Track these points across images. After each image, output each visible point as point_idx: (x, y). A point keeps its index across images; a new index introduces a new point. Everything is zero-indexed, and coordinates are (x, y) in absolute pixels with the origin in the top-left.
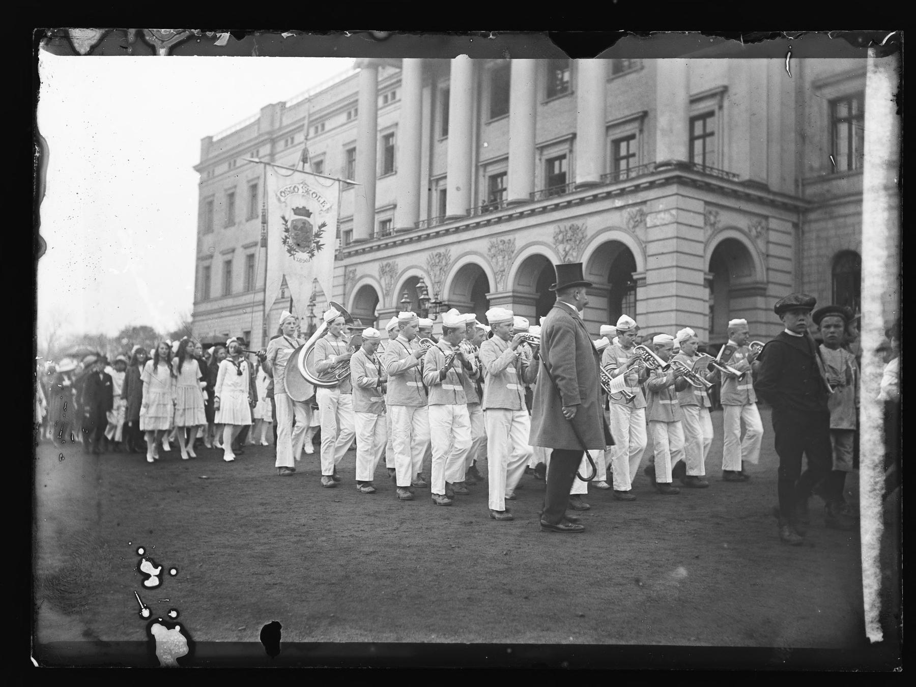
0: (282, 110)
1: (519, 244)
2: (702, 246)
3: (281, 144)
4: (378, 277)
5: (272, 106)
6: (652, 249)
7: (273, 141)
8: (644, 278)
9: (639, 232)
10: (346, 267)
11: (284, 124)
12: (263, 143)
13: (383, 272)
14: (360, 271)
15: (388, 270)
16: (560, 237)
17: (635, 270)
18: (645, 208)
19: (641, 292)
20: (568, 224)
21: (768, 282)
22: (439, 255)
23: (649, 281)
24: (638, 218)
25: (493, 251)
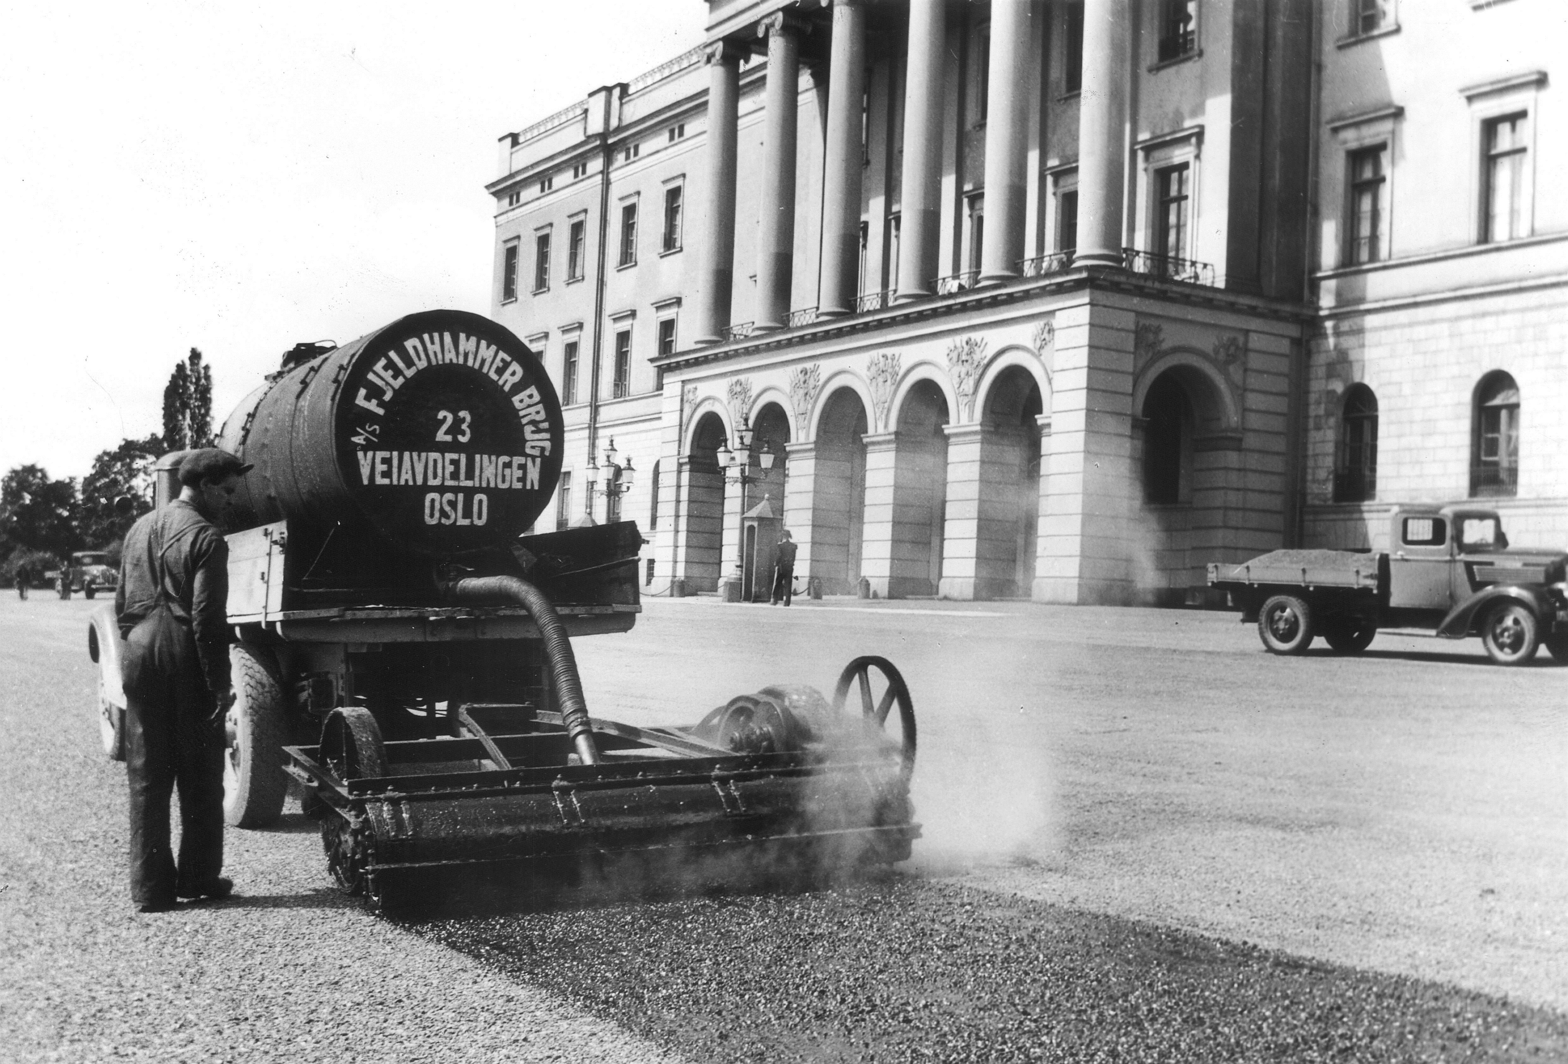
0: (621, 98)
2: (1130, 379)
3: (621, 158)
4: (726, 402)
5: (608, 90)
6: (1058, 379)
10: (683, 382)
11: (626, 121)
13: (733, 394)
14: (704, 390)
15: (739, 392)
16: (954, 355)
17: (1041, 412)
21: (1245, 430)
22: (805, 372)
24: (1046, 335)
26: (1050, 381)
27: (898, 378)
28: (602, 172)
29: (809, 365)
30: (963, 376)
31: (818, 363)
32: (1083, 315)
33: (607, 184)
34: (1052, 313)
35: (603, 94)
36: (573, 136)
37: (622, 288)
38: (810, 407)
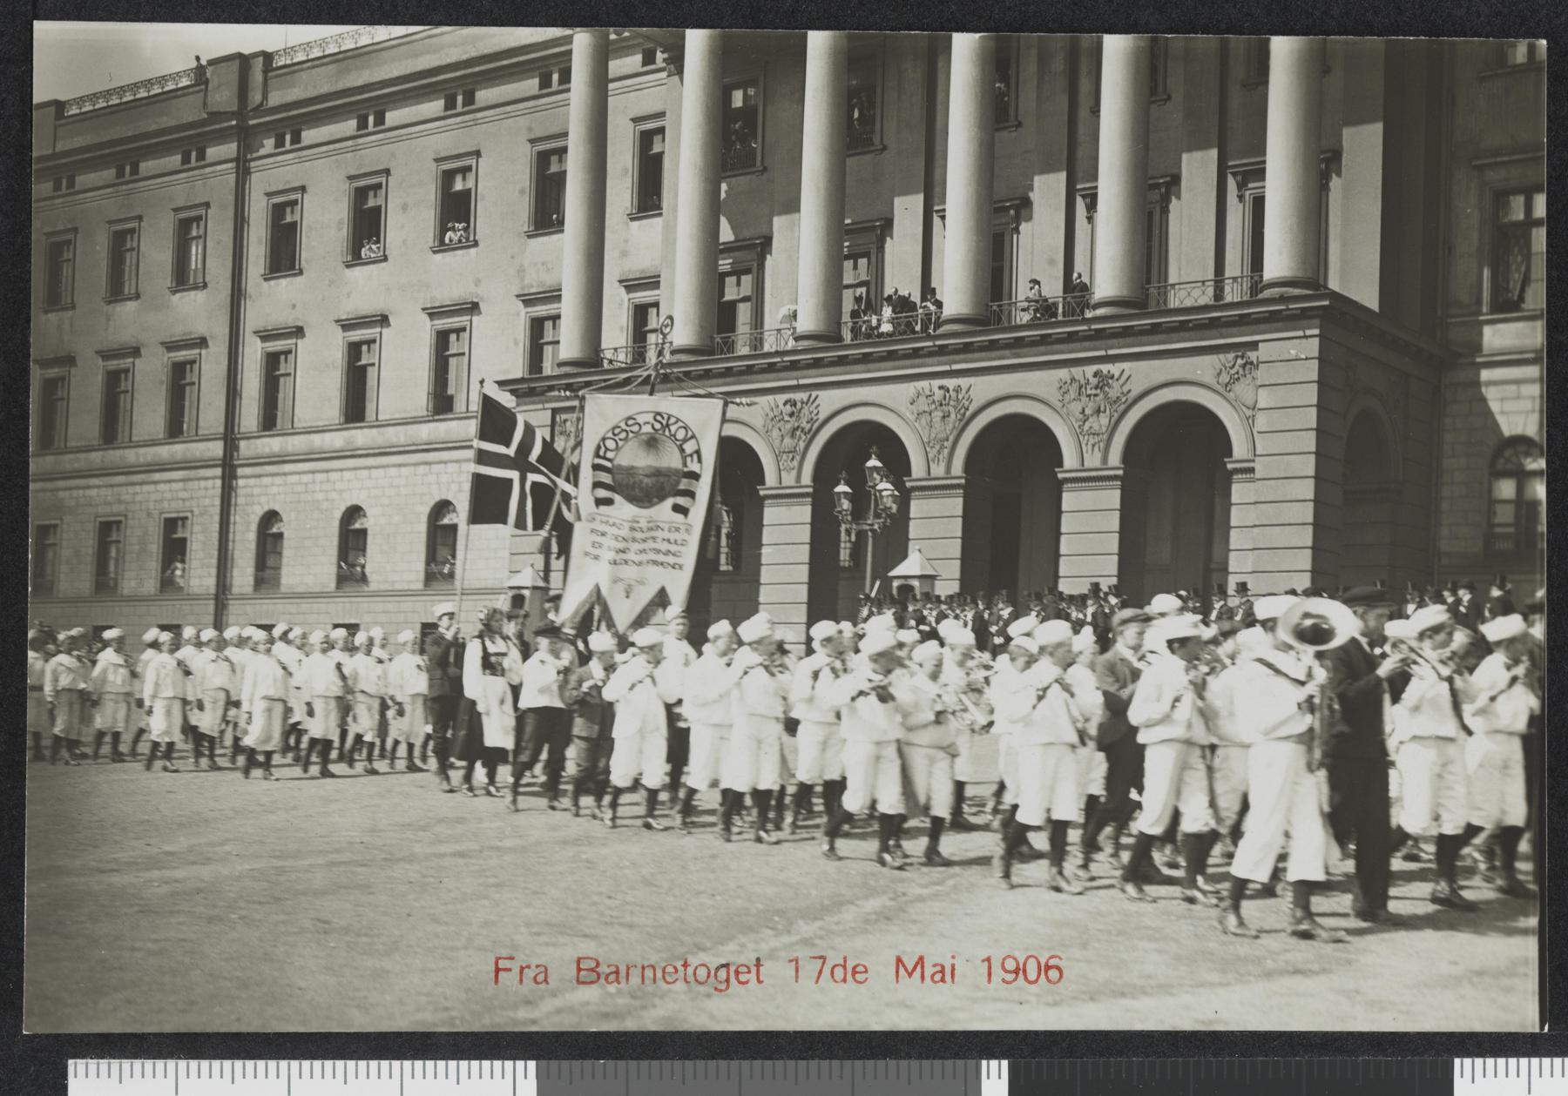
1: (978, 400)
3: (269, 144)
6: (1262, 422)
7: (247, 138)
8: (1252, 470)
9: (1243, 390)
10: (555, 411)
11: (275, 99)
12: (221, 137)
18: (1252, 356)
19: (1238, 492)
20: (1090, 370)
23: (1258, 475)
25: (923, 404)
26: (1250, 421)
27: (968, 413)
28: (237, 160)
29: (803, 396)
30: (1088, 412)
31: (814, 394)
32: (1312, 347)
33: (243, 173)
34: (1254, 345)
35: (237, 62)
36: (188, 111)
37: (272, 301)
38: (802, 445)
